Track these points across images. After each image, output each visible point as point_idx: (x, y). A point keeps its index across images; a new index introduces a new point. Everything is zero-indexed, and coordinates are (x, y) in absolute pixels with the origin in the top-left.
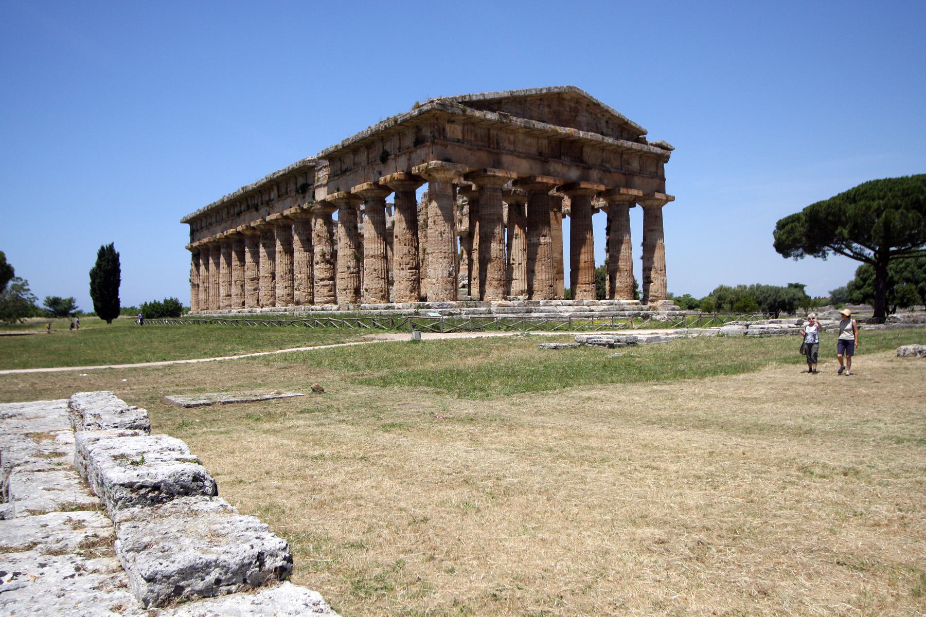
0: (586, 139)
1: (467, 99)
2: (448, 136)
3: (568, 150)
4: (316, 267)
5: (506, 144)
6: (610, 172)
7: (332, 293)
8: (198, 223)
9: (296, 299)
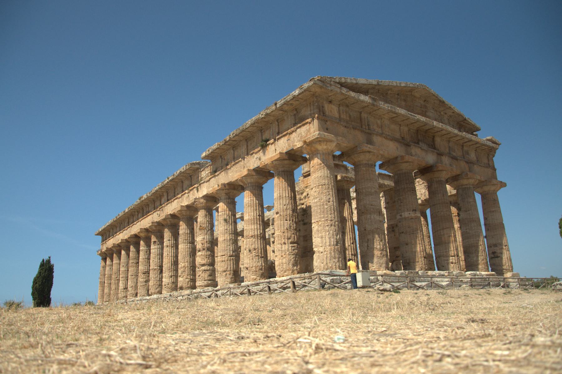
0: (438, 128)
1: (343, 80)
2: (327, 113)
3: (423, 137)
4: (199, 254)
5: (375, 127)
6: (457, 160)
7: (211, 278)
8: (105, 234)
9: (179, 285)
